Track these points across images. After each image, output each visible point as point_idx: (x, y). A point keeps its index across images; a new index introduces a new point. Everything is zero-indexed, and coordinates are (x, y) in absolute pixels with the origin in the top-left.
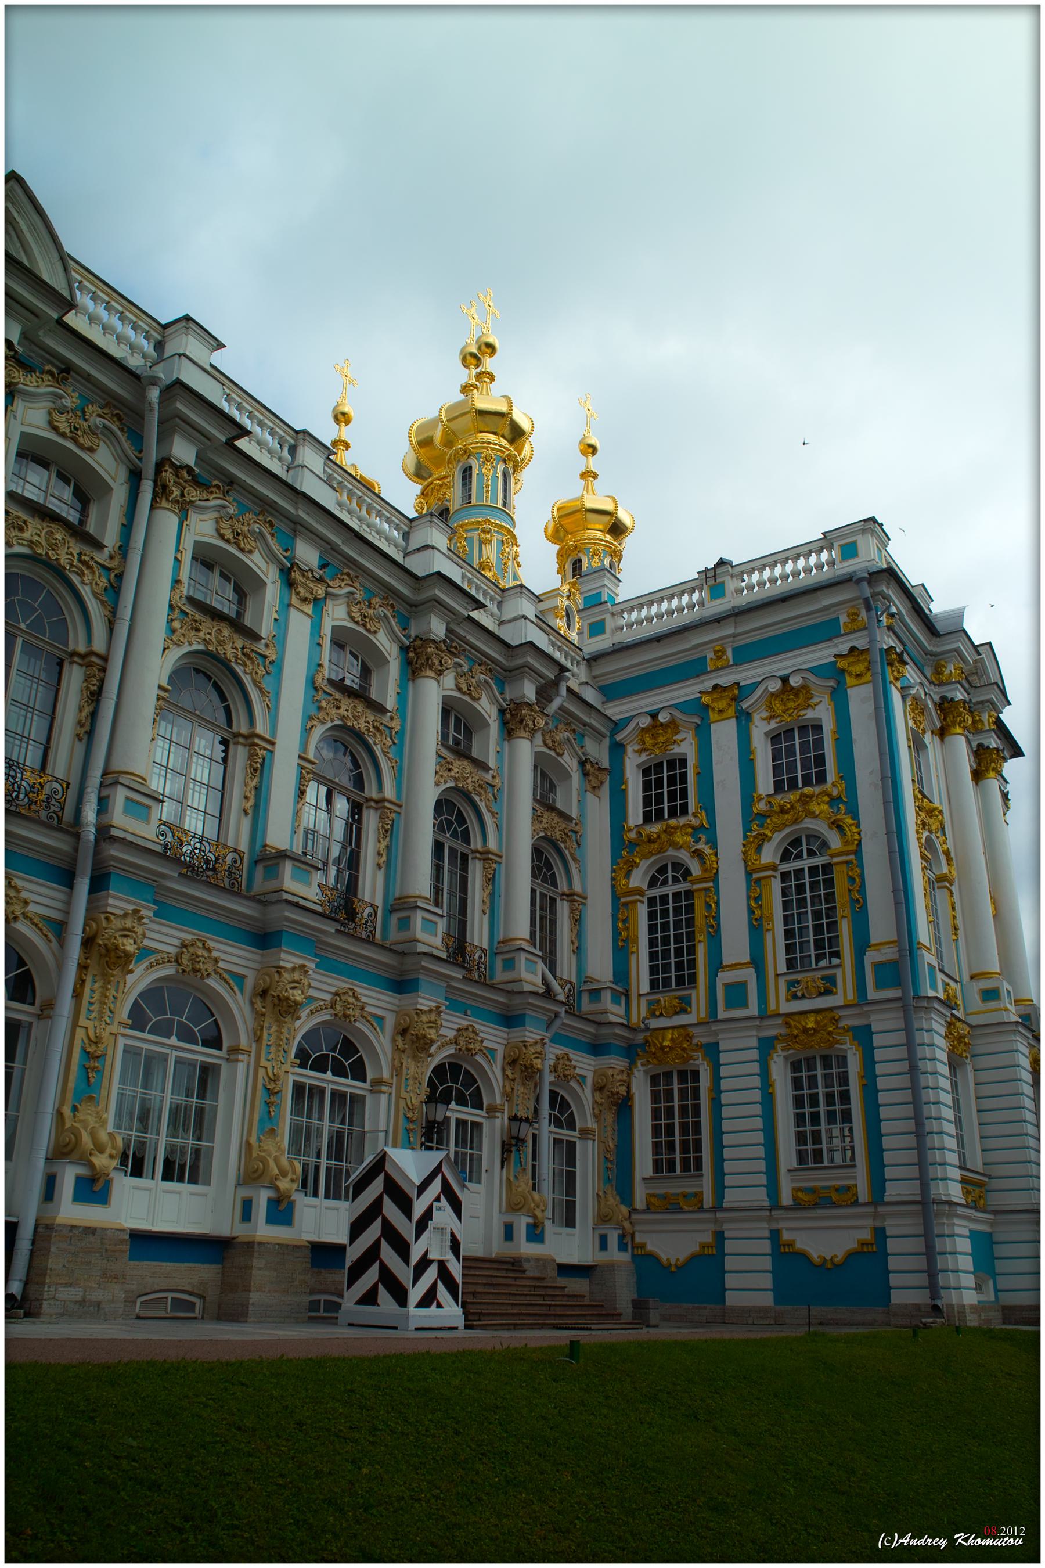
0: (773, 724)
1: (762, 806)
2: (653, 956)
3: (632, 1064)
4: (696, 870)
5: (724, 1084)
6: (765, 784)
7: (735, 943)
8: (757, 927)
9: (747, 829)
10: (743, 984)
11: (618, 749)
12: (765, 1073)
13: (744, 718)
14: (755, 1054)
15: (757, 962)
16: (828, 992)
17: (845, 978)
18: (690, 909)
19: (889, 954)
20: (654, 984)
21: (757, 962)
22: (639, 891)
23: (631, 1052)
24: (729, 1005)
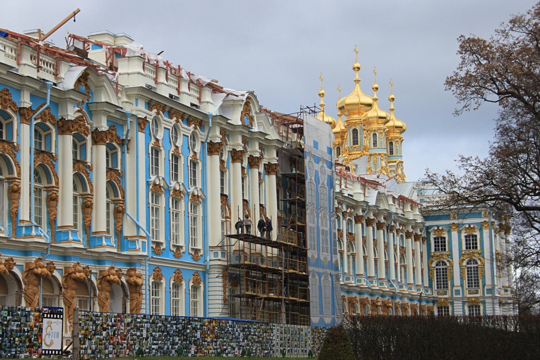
0: (466, 234)
1: (463, 252)
2: (437, 282)
3: (434, 305)
4: (448, 264)
5: (455, 310)
6: (464, 248)
7: (457, 281)
8: (462, 278)
9: (460, 257)
10: (459, 290)
11: (428, 233)
12: (463, 308)
13: (460, 232)
14: (461, 305)
15: (462, 285)
16: (477, 293)
17: (480, 291)
18: (446, 272)
19: (490, 287)
20: (438, 288)
21: (462, 285)
22: (434, 267)
23: (434, 302)
24: (456, 294)
